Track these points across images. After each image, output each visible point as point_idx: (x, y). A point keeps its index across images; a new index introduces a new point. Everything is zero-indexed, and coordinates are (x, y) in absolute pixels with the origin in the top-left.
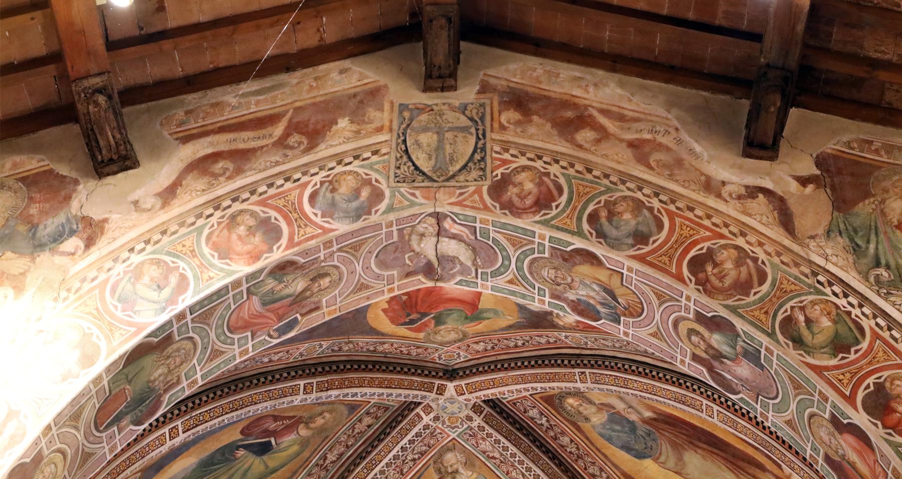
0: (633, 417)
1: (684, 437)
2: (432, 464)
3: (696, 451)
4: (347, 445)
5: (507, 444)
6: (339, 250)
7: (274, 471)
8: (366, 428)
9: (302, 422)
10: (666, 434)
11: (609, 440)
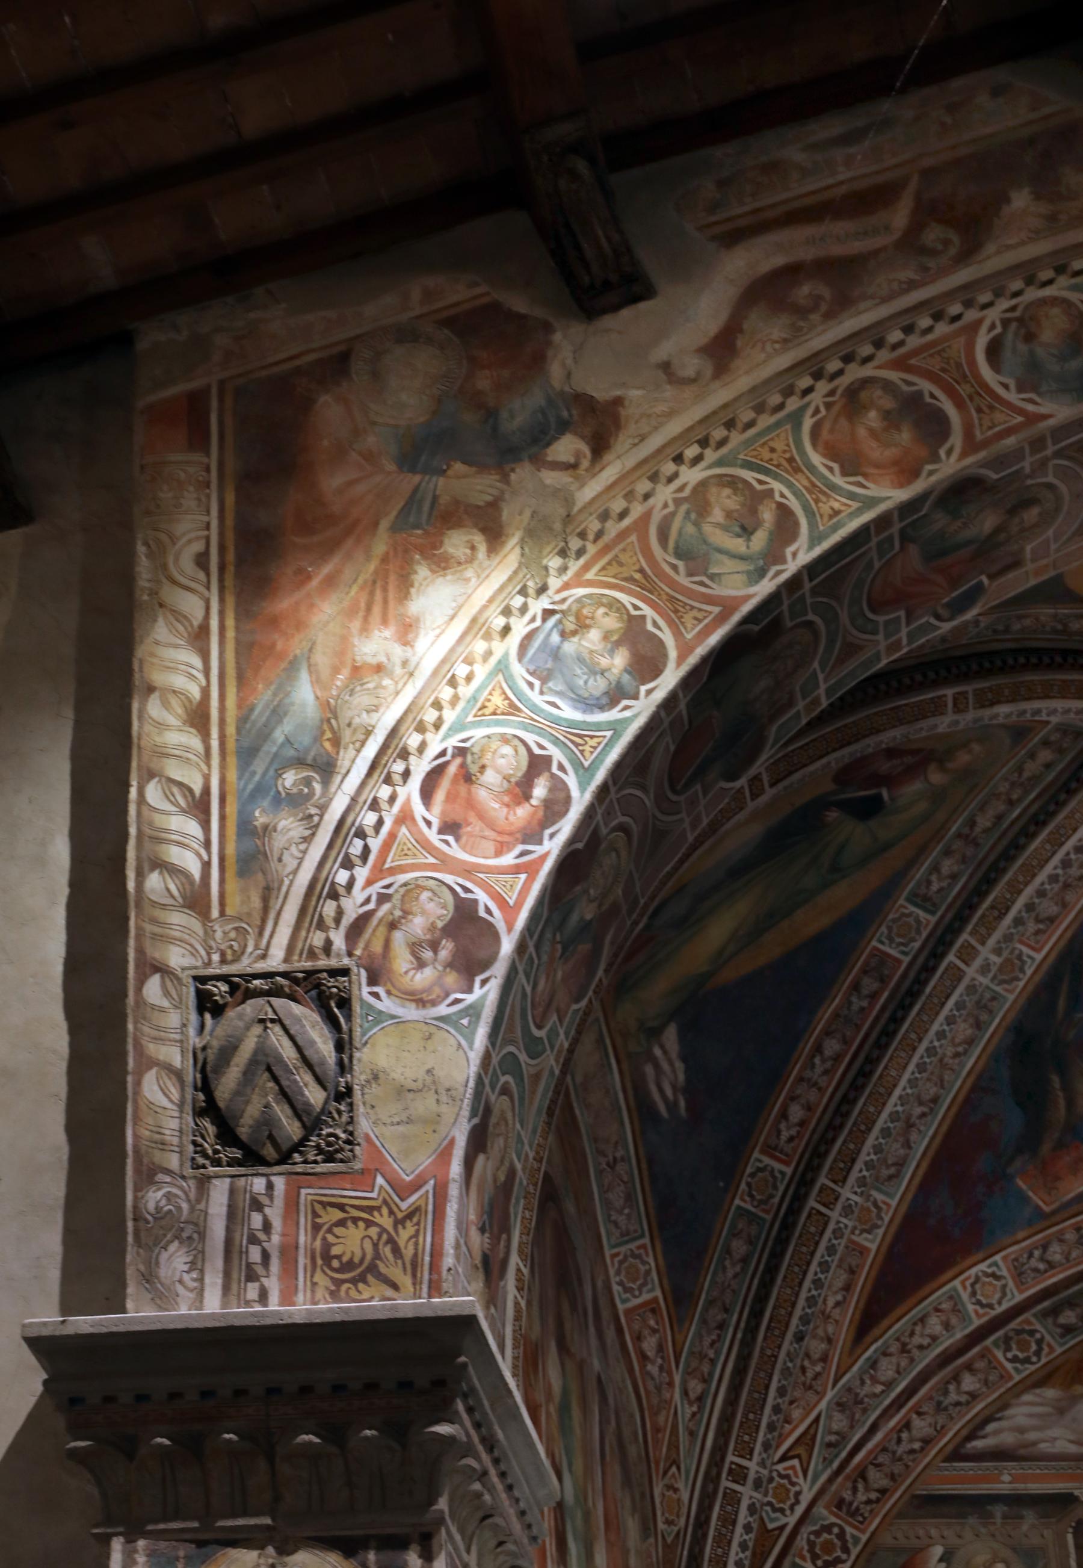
6: (1058, 454)
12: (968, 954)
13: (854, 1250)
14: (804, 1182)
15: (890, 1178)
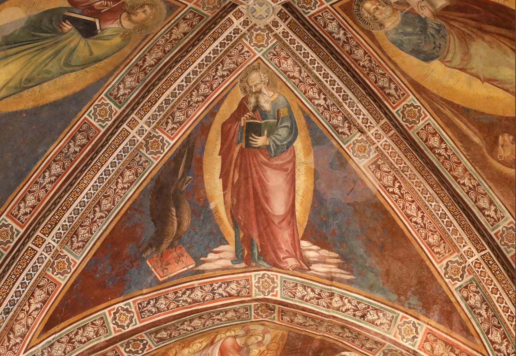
0: (426, 13)
1: (473, 23)
2: (239, 83)
3: (483, 39)
4: (164, 50)
5: (308, 50)
7: (98, 60)
8: (182, 35)
9: (125, 11)
10: (456, 24)
11: (400, 46)
12: (133, 124)
13: (51, 282)
14: (27, 236)
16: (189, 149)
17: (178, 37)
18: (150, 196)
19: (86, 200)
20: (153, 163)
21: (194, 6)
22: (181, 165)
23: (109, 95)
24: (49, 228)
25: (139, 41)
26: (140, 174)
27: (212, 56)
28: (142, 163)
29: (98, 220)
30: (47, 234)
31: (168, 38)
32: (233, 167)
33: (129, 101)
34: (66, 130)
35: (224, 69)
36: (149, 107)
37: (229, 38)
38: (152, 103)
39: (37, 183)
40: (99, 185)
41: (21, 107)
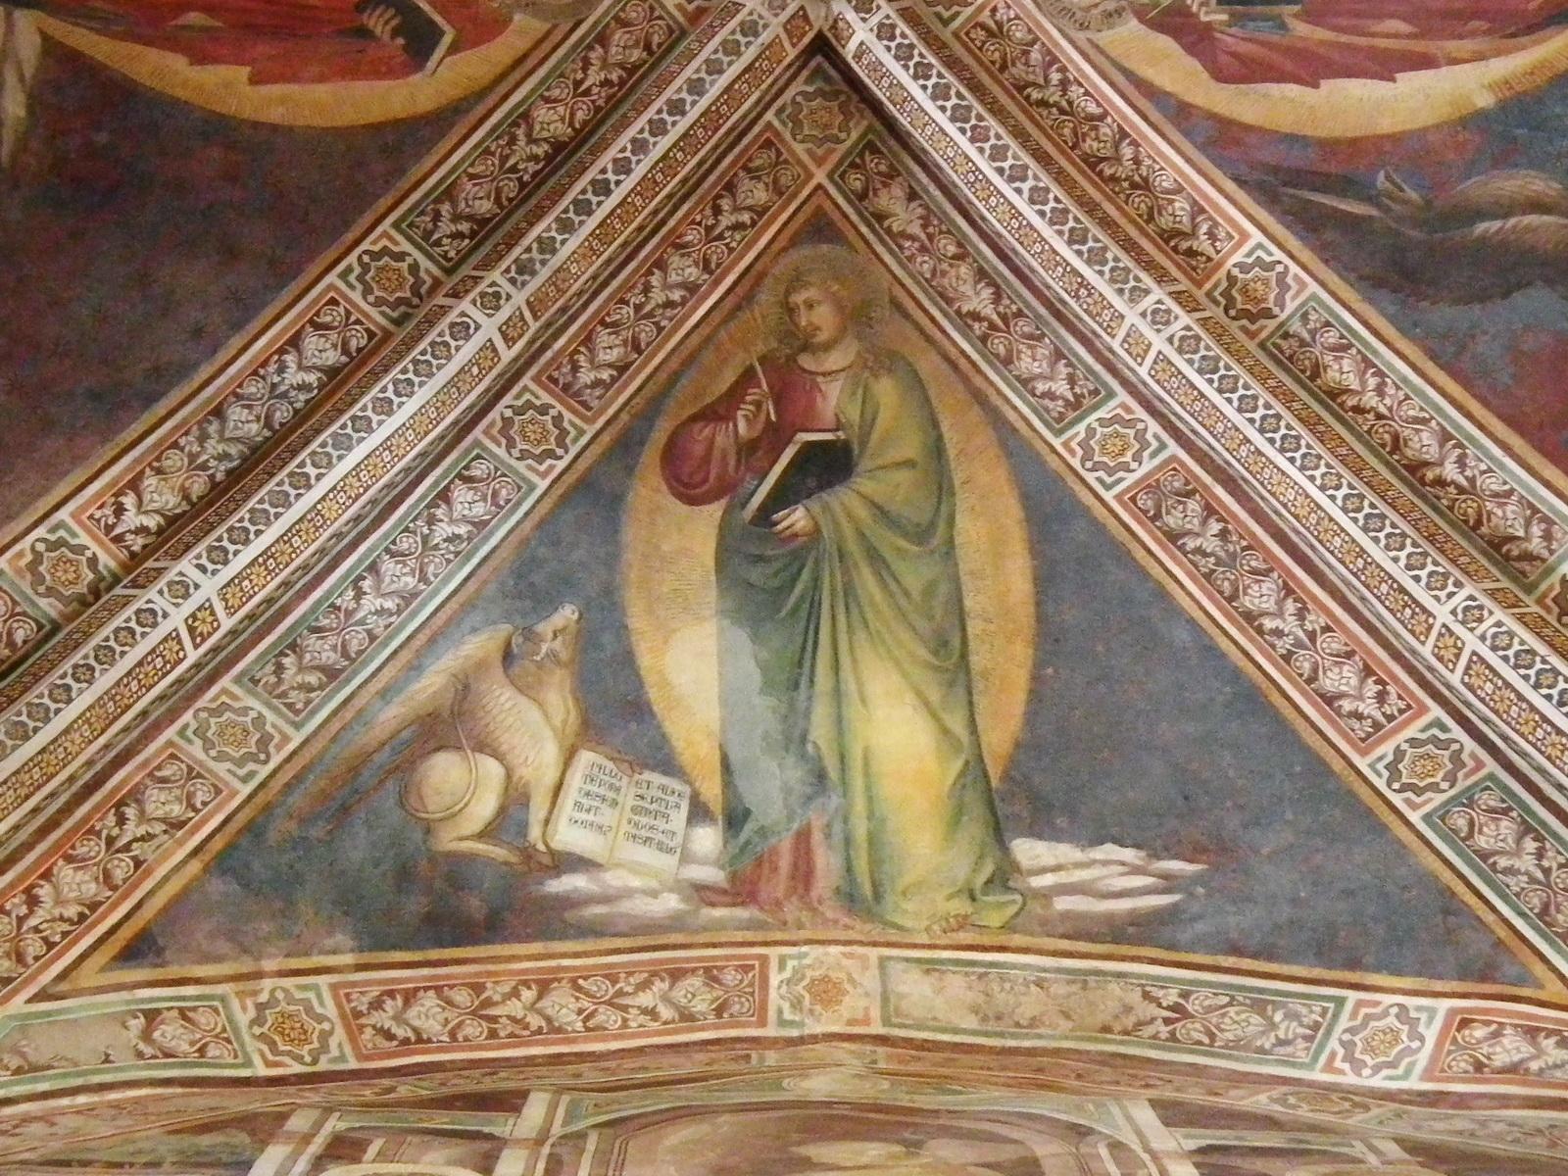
2: (1089, 34)
4: (955, 257)
7: (937, 450)
8: (913, 205)
9: (792, 359)
12: (1137, 345)
15: (1547, 536)
16: (1285, 185)
17: (921, 218)
18: (1425, 304)
19: (1345, 490)
20: (1314, 297)
21: (829, 166)
22: (1336, 210)
23: (1060, 424)
24: (1414, 613)
25: (908, 327)
26: (1342, 337)
27: (954, 101)
28: (1310, 332)
29: (1468, 473)
30: (1426, 621)
31: (917, 245)
32: (1362, 41)
33: (1098, 368)
34: (1140, 554)
35: (1041, 81)
36: (1090, 295)
37: (904, 55)
38: (1080, 285)
39: (1287, 657)
40: (1303, 450)
41: (1020, 680)
